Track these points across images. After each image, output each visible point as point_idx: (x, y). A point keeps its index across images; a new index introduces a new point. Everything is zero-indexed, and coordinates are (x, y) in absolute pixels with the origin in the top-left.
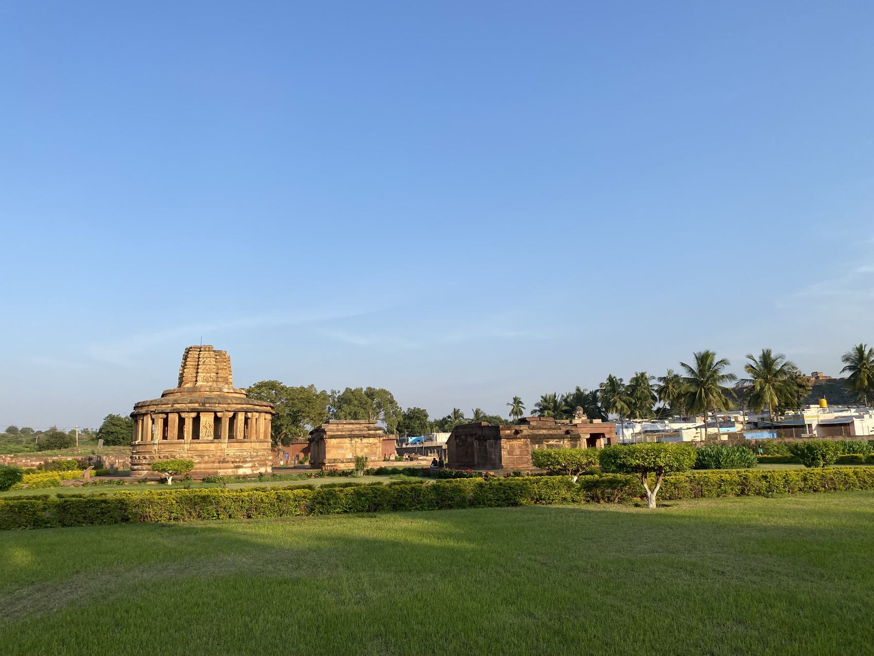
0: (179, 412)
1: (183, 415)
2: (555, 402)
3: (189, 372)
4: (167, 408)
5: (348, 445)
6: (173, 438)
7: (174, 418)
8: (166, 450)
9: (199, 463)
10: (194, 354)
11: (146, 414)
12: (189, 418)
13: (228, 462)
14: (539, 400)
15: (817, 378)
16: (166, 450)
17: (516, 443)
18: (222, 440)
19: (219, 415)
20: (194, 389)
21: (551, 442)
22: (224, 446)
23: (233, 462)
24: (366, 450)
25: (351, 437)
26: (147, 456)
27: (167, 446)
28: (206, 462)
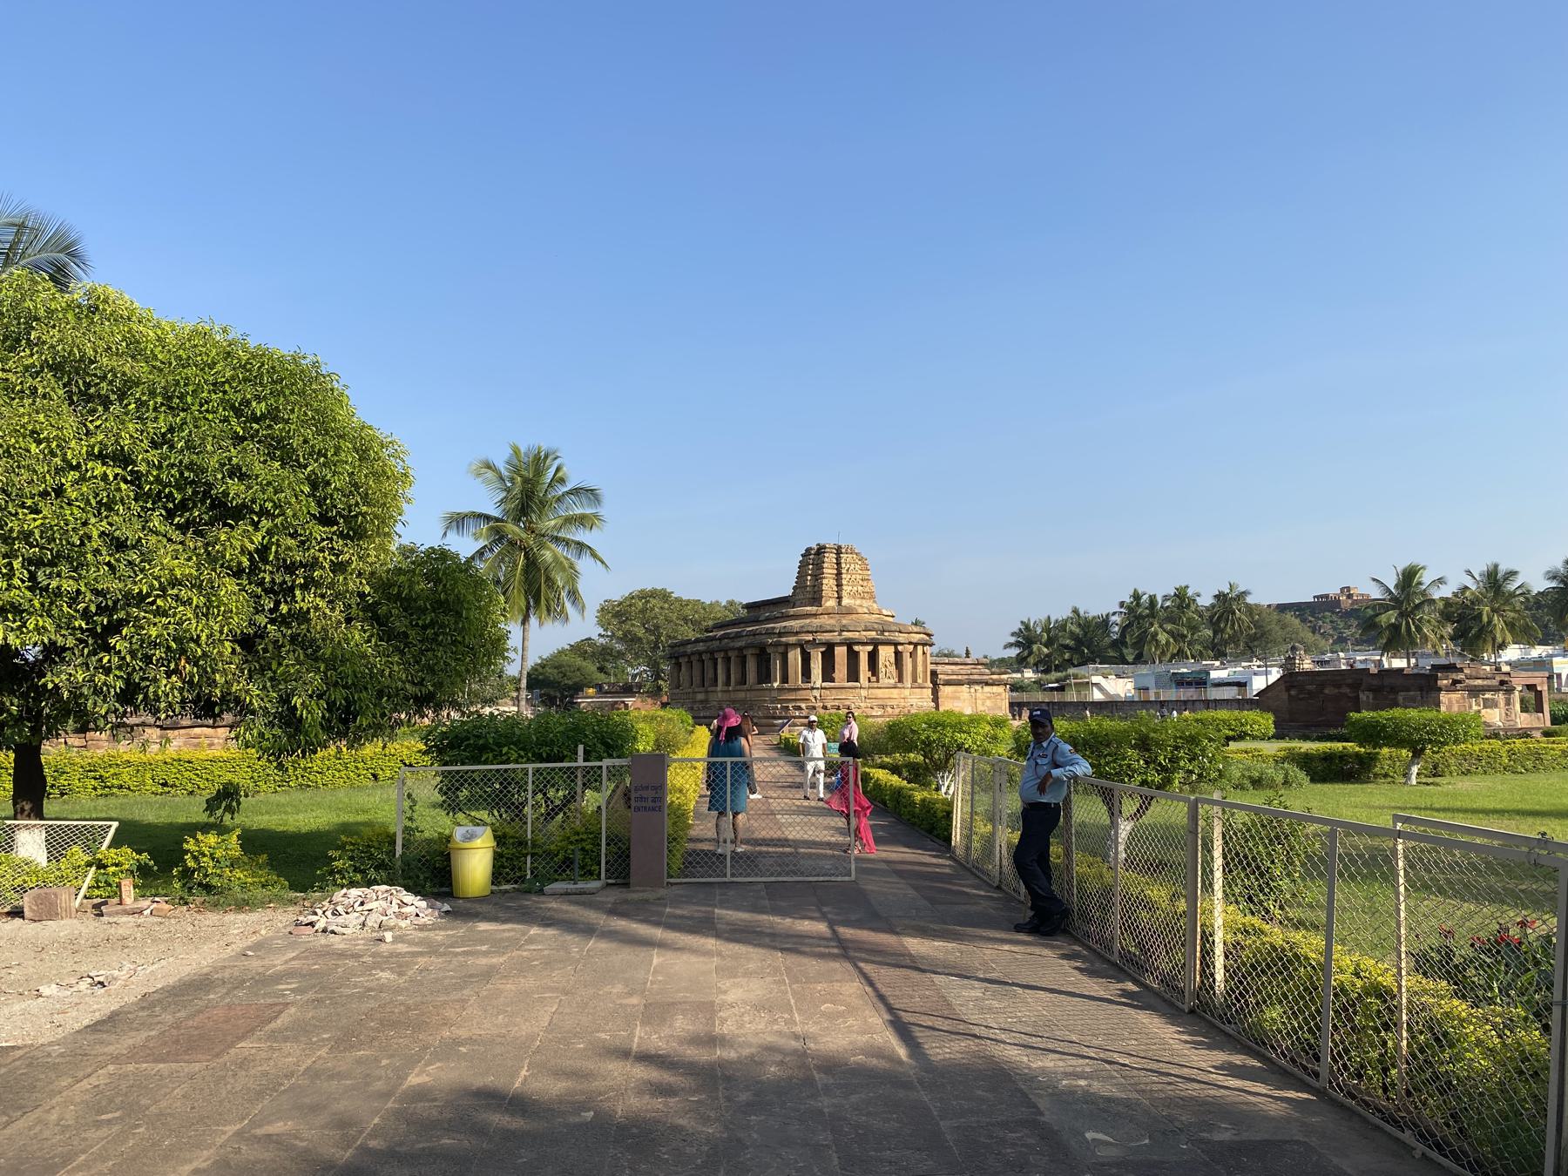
1: (856, 648)
2: (1048, 630)
3: (828, 584)
5: (966, 695)
7: (841, 652)
8: (831, 698)
10: (830, 558)
11: (794, 645)
12: (864, 652)
14: (1017, 627)
15: (1350, 596)
16: (831, 698)
17: (1455, 696)
20: (850, 611)
21: (1487, 696)
22: (907, 692)
24: (988, 703)
25: (971, 683)
26: (803, 706)
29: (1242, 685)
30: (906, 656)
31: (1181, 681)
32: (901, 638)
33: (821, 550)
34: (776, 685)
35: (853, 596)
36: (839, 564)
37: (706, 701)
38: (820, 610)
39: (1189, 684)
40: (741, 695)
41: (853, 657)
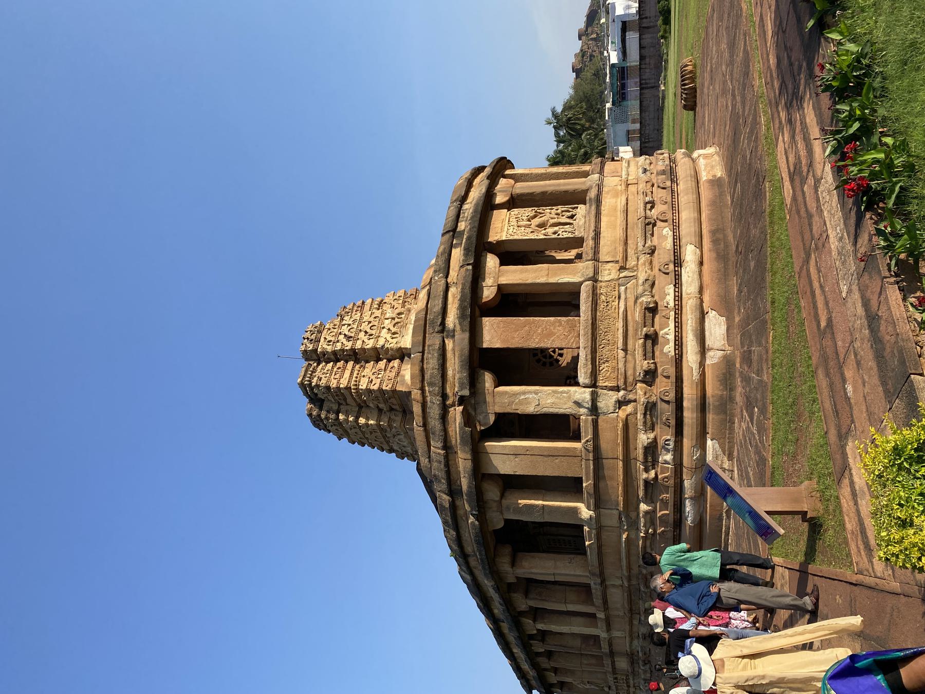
0: (476, 309)
1: (488, 293)
3: (370, 377)
4: (456, 349)
6: (573, 327)
9: (676, 227)
11: (478, 456)
22: (611, 182)
29: (625, 27)
30: (522, 188)
31: (621, 96)
32: (476, 193)
33: (317, 396)
34: (585, 513)
35: (398, 321)
36: (335, 357)
37: (632, 657)
38: (416, 394)
39: (623, 86)
40: (617, 597)
41: (512, 302)
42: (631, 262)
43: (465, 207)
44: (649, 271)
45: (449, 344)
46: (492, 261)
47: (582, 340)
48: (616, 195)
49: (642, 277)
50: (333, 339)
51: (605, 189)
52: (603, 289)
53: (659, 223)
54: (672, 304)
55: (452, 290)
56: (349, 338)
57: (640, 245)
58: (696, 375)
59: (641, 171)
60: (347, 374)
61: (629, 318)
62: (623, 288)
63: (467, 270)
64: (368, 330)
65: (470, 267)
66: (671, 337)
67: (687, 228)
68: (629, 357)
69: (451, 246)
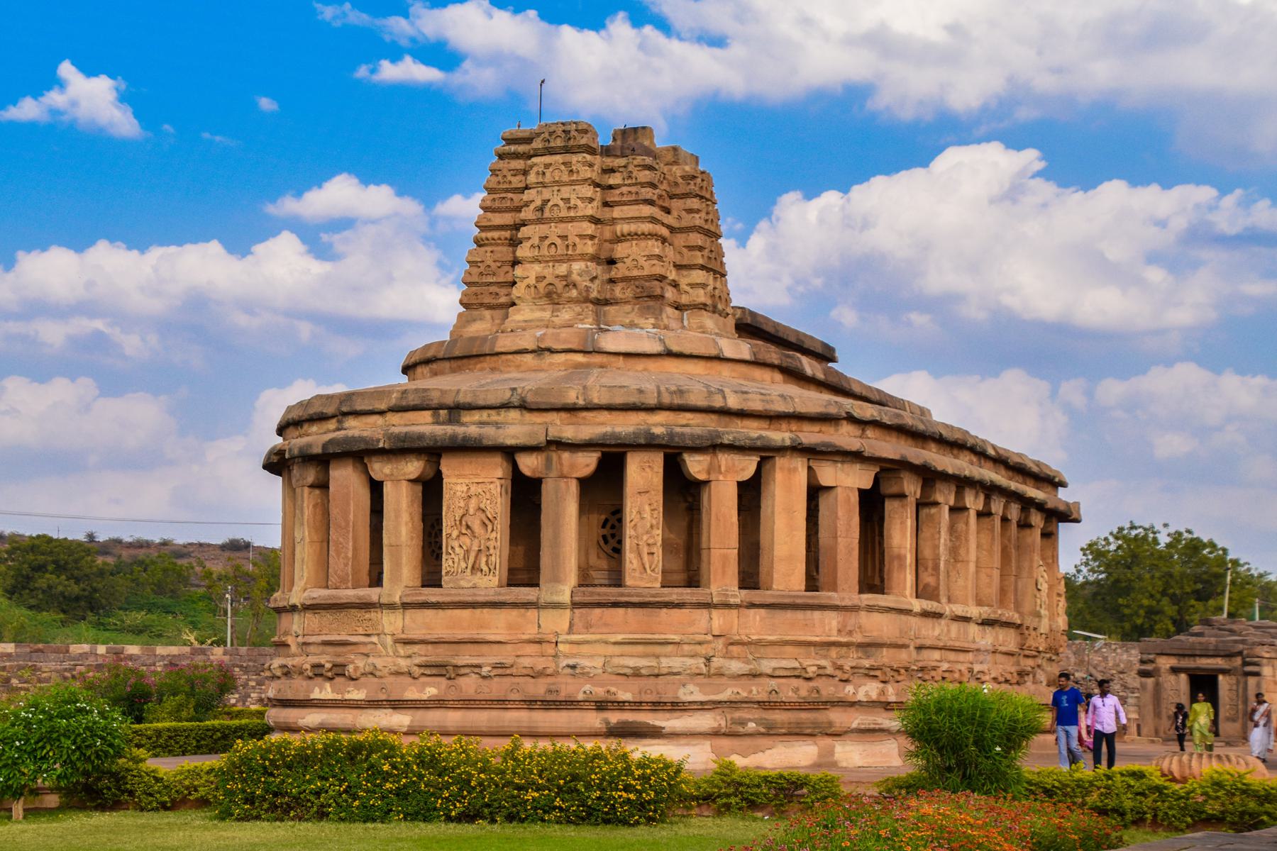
6: (343, 580)
13: (570, 704)
18: (544, 593)
19: (528, 464)
22: (556, 622)
23: (601, 706)
27: (328, 617)
28: (468, 704)
32: (515, 429)
42: (402, 650)
43: (514, 415)
44: (386, 670)
45: (332, 424)
46: (414, 467)
47: (333, 592)
48: (510, 627)
49: (379, 663)
50: (548, 178)
51: (532, 614)
52: (373, 615)
53: (443, 680)
54: (347, 696)
55: (378, 420)
56: (541, 209)
57: (418, 660)
58: (302, 722)
59: (571, 662)
60: (498, 219)
61: (349, 648)
62: (374, 639)
63: (378, 441)
64: (547, 242)
65: (381, 445)
66: (322, 696)
67: (434, 718)
68: (321, 648)
69: (436, 409)
